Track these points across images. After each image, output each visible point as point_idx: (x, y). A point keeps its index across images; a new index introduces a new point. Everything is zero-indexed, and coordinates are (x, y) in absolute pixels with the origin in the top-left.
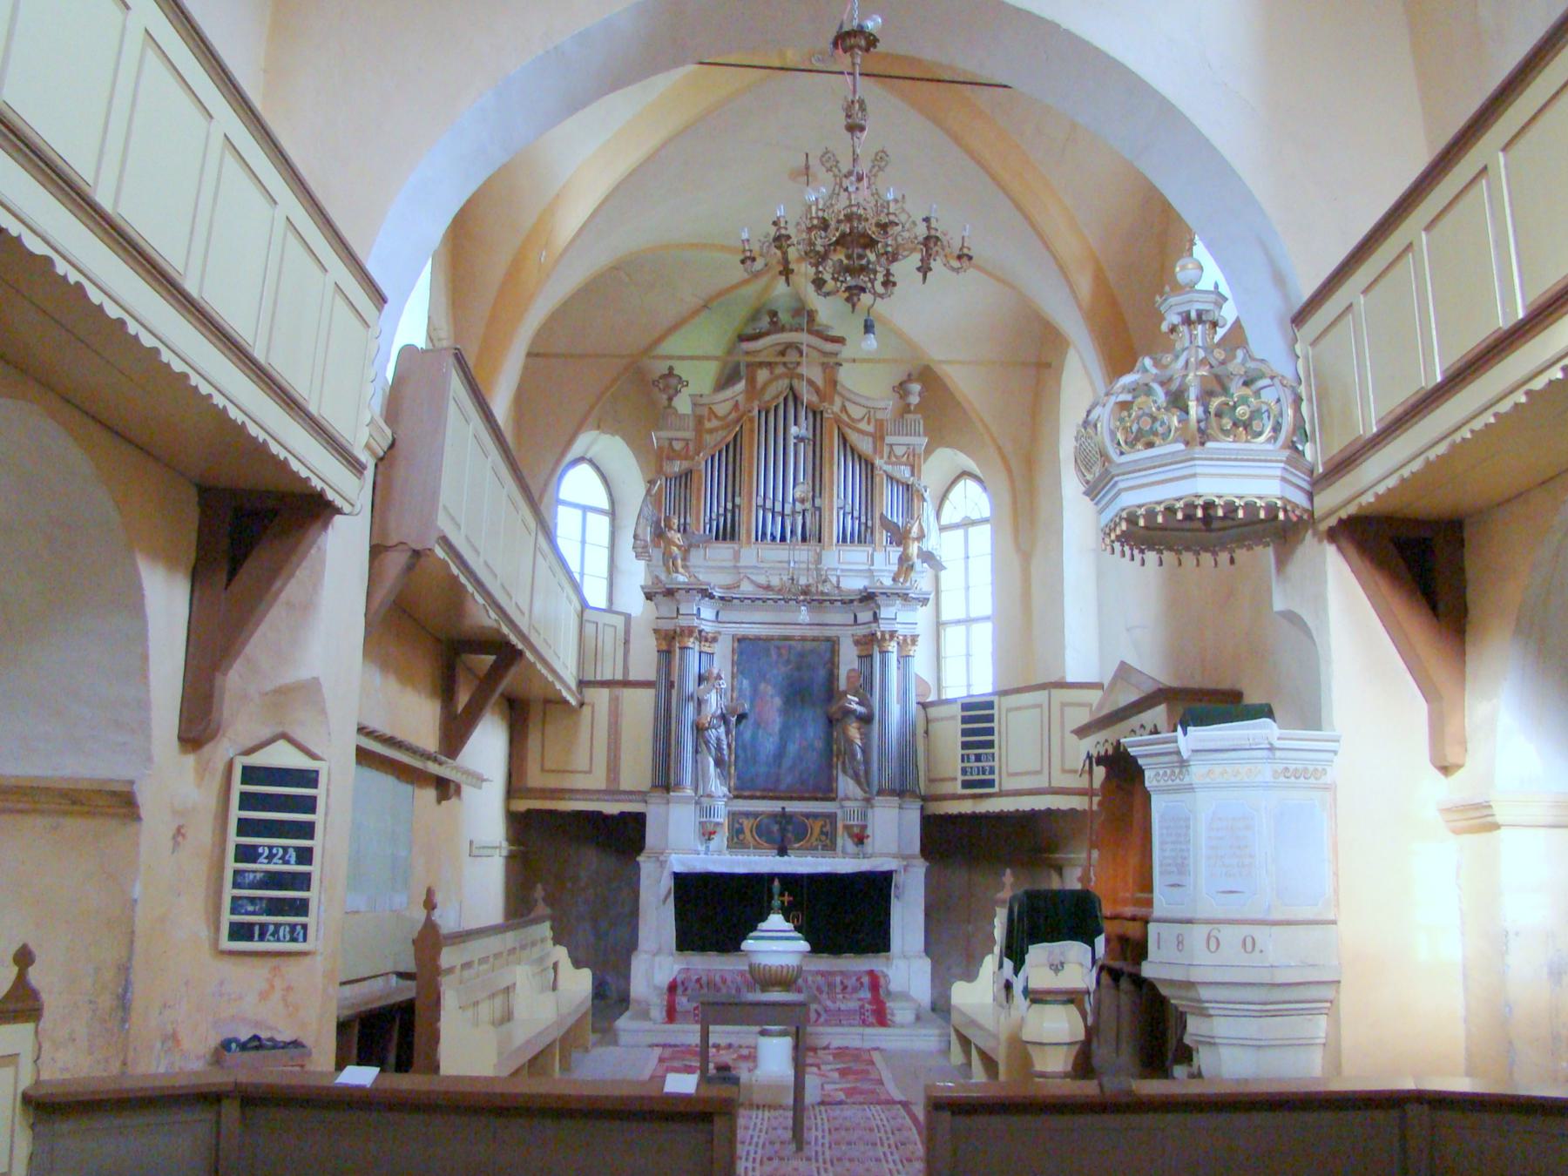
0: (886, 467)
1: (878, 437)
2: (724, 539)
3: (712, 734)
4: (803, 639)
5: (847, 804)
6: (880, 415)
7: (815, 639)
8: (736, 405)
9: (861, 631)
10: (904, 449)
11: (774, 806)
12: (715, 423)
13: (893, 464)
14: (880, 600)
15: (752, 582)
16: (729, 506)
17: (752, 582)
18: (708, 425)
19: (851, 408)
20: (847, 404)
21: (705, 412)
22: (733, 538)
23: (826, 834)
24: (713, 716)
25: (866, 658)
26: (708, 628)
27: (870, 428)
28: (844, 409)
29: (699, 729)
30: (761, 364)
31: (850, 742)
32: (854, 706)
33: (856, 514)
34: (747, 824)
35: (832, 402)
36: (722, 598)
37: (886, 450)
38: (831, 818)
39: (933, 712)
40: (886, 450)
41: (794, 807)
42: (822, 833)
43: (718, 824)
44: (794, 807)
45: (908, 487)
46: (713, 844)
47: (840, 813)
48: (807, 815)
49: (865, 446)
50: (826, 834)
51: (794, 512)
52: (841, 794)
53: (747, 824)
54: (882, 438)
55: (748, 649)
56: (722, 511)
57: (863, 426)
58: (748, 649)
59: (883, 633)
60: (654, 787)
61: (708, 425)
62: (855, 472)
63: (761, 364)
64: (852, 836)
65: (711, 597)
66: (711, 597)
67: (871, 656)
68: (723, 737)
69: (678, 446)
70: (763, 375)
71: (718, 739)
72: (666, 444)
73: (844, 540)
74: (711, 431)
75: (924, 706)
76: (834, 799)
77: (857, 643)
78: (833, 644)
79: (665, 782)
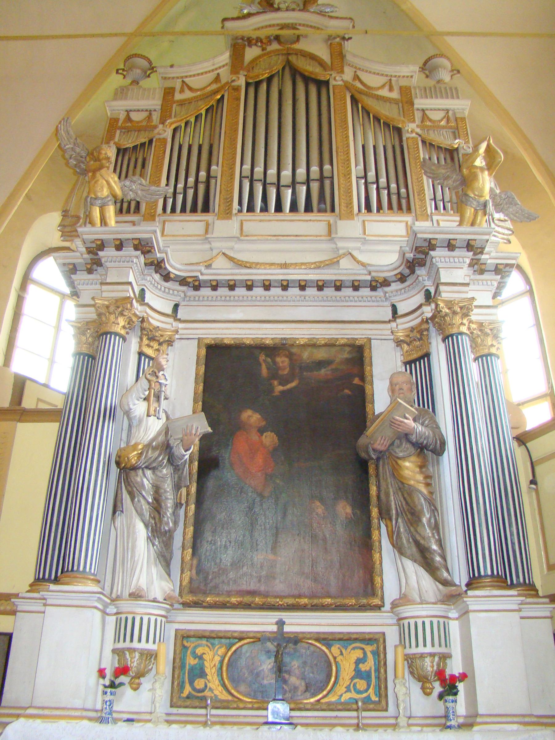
0: (418, 130)
1: (406, 100)
2: (194, 210)
3: (146, 480)
4: (312, 345)
5: (408, 611)
6: (404, 83)
7: (330, 344)
8: (217, 79)
9: (403, 325)
10: (442, 114)
11: (263, 622)
12: (188, 95)
13: (429, 128)
14: (439, 255)
15: (231, 259)
16: (203, 174)
17: (231, 259)
18: (178, 96)
19: (364, 76)
20: (359, 73)
21: (178, 85)
22: (206, 209)
23: (366, 676)
24: (148, 446)
25: (419, 361)
26: (155, 321)
27: (395, 95)
28: (356, 77)
29: (125, 470)
30: (250, 42)
31: (406, 491)
32: (410, 422)
33: (383, 181)
34: (212, 657)
35: (342, 72)
36: (183, 282)
37: (418, 116)
38: (375, 641)
39: (539, 447)
40: (418, 116)
41: (299, 623)
42: (358, 674)
43: (150, 656)
44: (299, 623)
45: (452, 153)
46: (129, 700)
47: (392, 637)
48: (327, 639)
49: (387, 112)
50: (366, 676)
51: (294, 184)
52: (390, 588)
53: (212, 657)
54: (412, 104)
55: (228, 370)
56: (191, 180)
57: (384, 92)
58: (228, 370)
59: (450, 304)
60: (40, 581)
61: (178, 96)
62: (376, 139)
63: (250, 42)
64: (422, 679)
65: (167, 277)
66: (167, 277)
67: (427, 355)
68: (168, 486)
69: (135, 117)
70: (251, 53)
71: (157, 490)
72: (122, 116)
73: (368, 208)
74: (182, 103)
75: (522, 439)
76: (378, 608)
77: (399, 343)
78: (358, 356)
79: (56, 565)
